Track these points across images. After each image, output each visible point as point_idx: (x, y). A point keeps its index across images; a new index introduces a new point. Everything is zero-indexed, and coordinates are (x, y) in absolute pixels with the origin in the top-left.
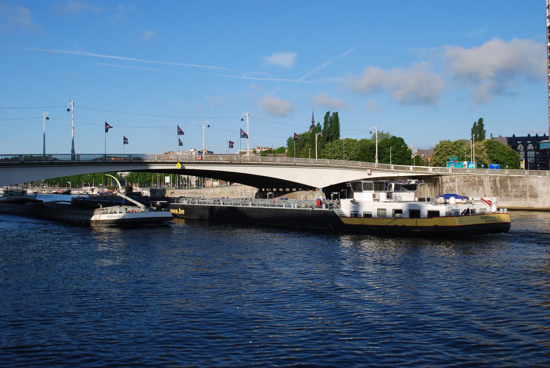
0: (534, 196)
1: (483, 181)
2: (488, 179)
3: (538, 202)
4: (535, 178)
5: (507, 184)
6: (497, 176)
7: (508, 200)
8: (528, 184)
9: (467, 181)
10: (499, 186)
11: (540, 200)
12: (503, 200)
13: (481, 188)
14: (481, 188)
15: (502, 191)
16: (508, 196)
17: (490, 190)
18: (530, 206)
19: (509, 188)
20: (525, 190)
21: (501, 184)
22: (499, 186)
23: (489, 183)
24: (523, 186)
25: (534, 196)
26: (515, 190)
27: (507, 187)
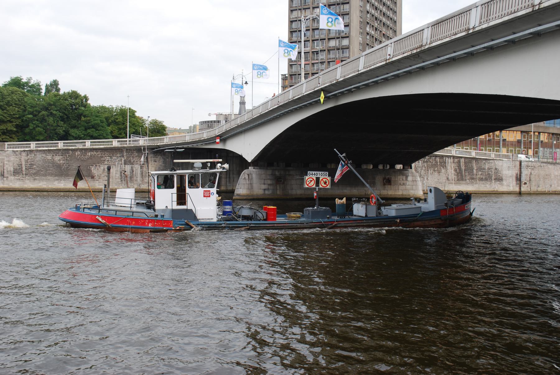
0: (499, 179)
3: (502, 185)
5: (472, 166)
6: (461, 157)
8: (494, 167)
9: (427, 162)
10: (463, 168)
11: (504, 183)
13: (443, 171)
14: (443, 171)
15: (467, 174)
17: (453, 172)
18: (495, 190)
19: (475, 171)
21: (465, 166)
22: (463, 168)
23: (453, 165)
24: (489, 169)
25: (499, 179)
26: (480, 173)
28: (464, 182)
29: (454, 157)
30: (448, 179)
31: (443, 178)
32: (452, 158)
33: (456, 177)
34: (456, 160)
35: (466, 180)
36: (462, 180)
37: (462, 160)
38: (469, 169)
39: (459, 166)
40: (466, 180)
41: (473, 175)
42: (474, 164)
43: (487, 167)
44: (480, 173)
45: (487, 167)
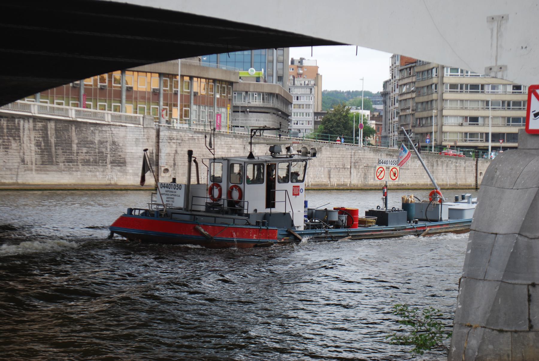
0: (120, 162)
1: (18, 129)
2: (31, 124)
3: (125, 173)
4: (122, 129)
5: (70, 137)
6: (50, 120)
7: (70, 169)
8: (110, 140)
10: (53, 140)
12: (61, 171)
13: (14, 145)
14: (14, 145)
15: (60, 152)
16: (71, 161)
17: (33, 147)
18: (113, 182)
19: (75, 147)
20: (104, 150)
21: (57, 137)
22: (53, 140)
23: (33, 134)
24: (101, 142)
25: (120, 162)
26: (85, 150)
27: (69, 143)
28: (55, 167)
29: (35, 119)
30: (23, 161)
31: (15, 161)
32: (31, 121)
33: (38, 157)
34: (39, 125)
35: (57, 163)
36: (51, 163)
37: (51, 126)
38: (64, 143)
39: (45, 137)
40: (57, 163)
41: (71, 153)
42: (74, 134)
43: (97, 138)
44: (85, 150)
45: (97, 138)
